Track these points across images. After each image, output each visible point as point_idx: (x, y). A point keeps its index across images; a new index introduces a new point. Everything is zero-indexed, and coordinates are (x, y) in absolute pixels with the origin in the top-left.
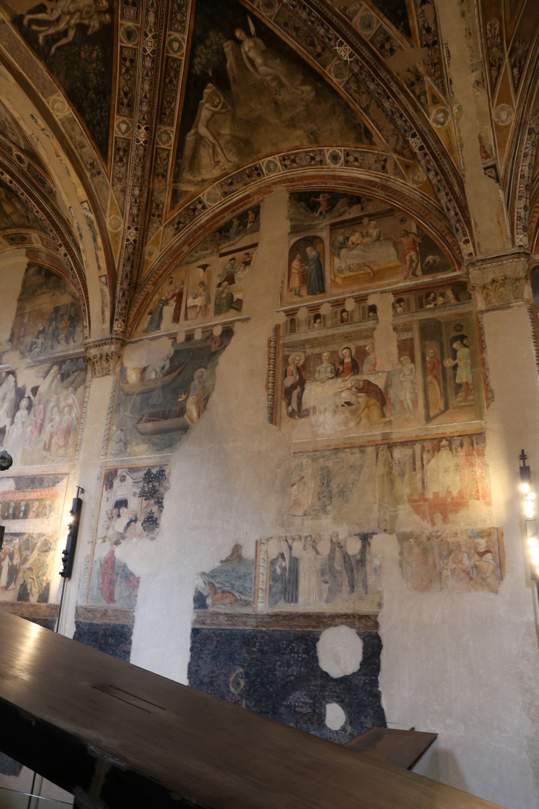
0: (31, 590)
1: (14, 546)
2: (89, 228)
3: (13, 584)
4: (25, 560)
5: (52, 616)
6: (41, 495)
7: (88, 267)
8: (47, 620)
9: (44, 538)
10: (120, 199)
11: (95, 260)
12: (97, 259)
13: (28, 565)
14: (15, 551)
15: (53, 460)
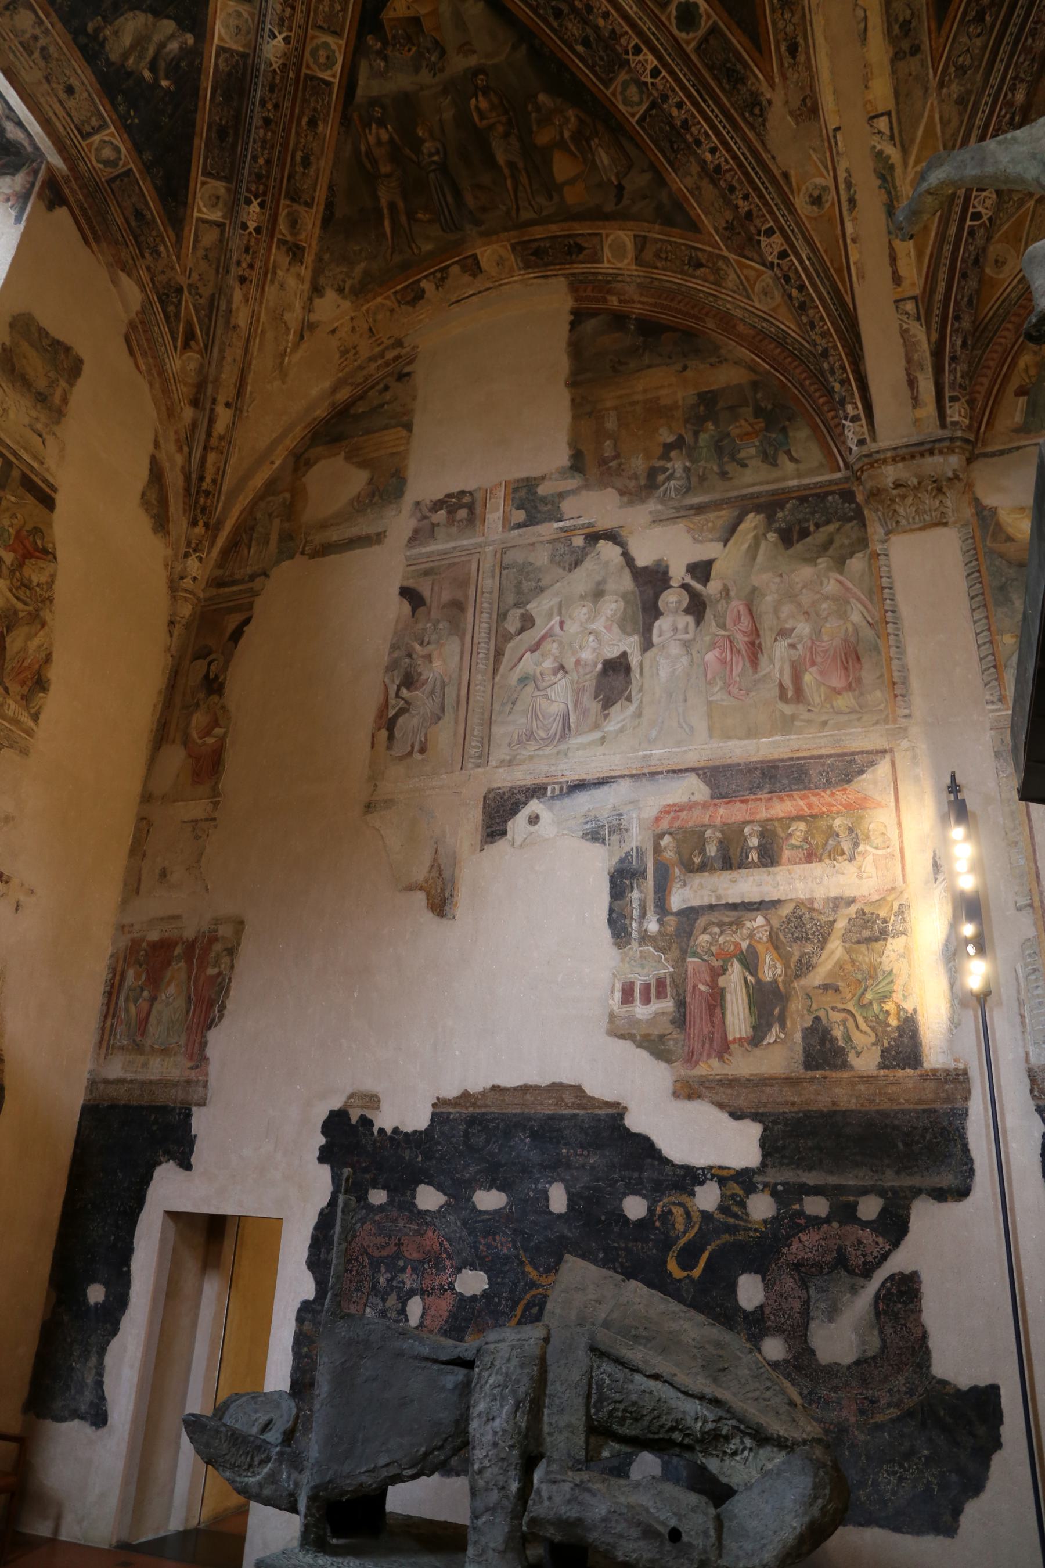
0: (848, 1039)
1: (751, 936)
2: (879, 182)
3: (775, 1029)
4: (804, 967)
5: (947, 1100)
6: (810, 806)
7: (862, 276)
8: (935, 1111)
9: (853, 909)
10: (949, 121)
11: (886, 260)
12: (893, 259)
13: (817, 977)
14: (760, 948)
15: (825, 723)
